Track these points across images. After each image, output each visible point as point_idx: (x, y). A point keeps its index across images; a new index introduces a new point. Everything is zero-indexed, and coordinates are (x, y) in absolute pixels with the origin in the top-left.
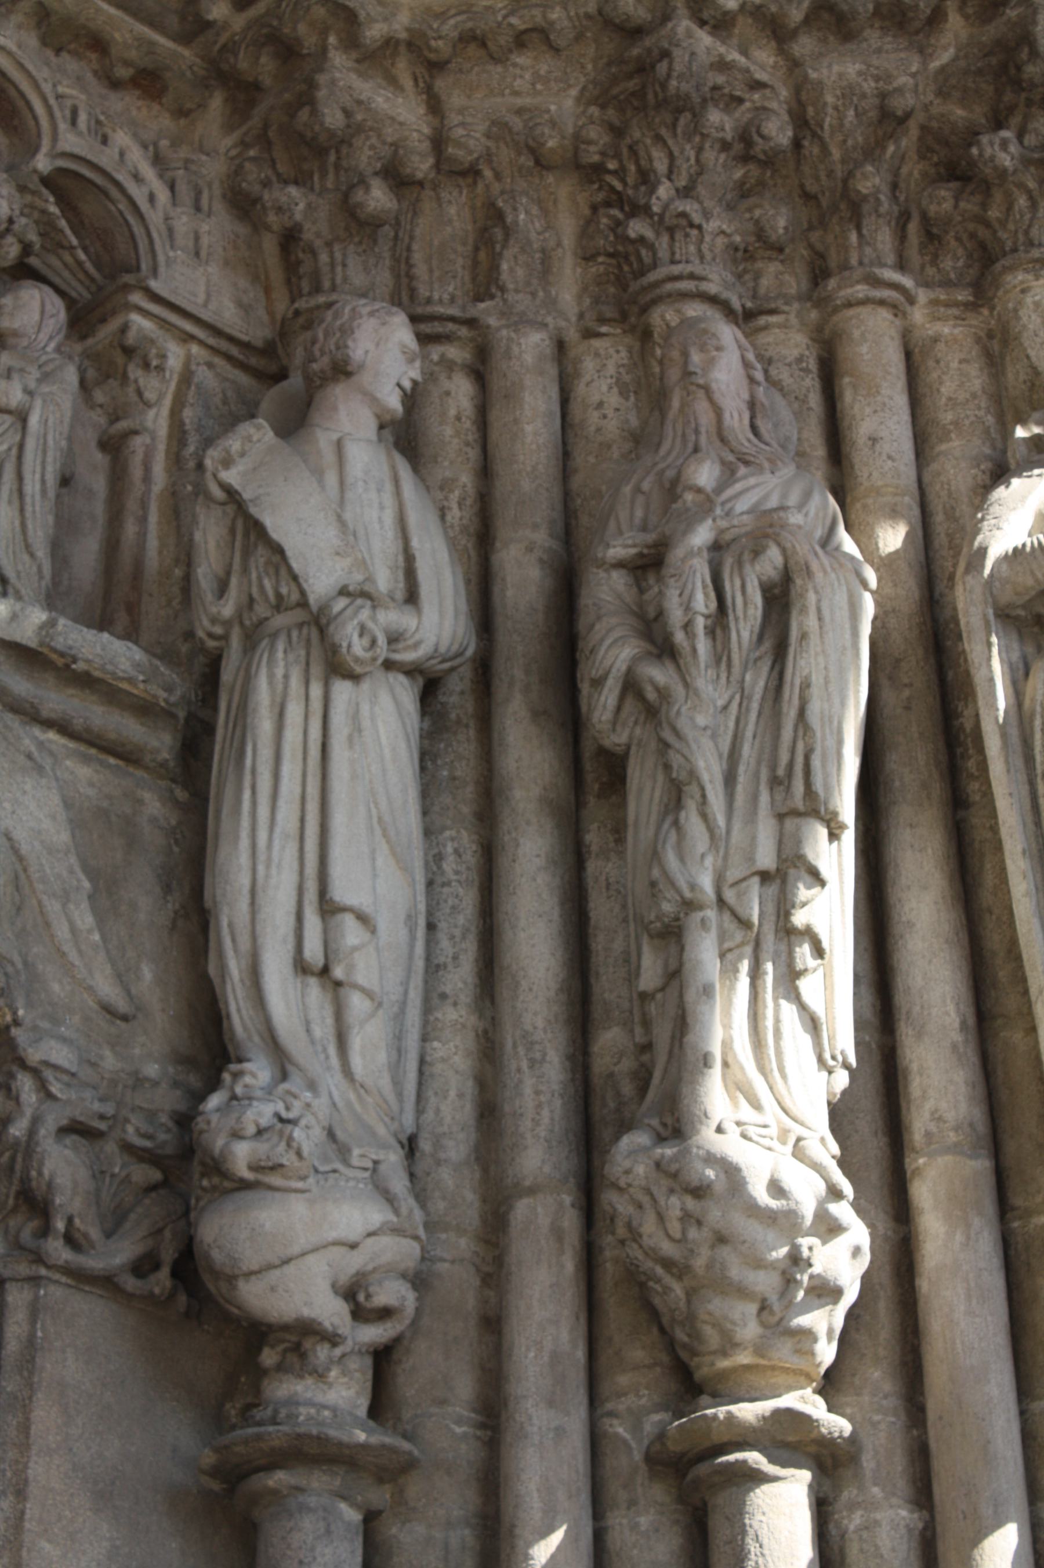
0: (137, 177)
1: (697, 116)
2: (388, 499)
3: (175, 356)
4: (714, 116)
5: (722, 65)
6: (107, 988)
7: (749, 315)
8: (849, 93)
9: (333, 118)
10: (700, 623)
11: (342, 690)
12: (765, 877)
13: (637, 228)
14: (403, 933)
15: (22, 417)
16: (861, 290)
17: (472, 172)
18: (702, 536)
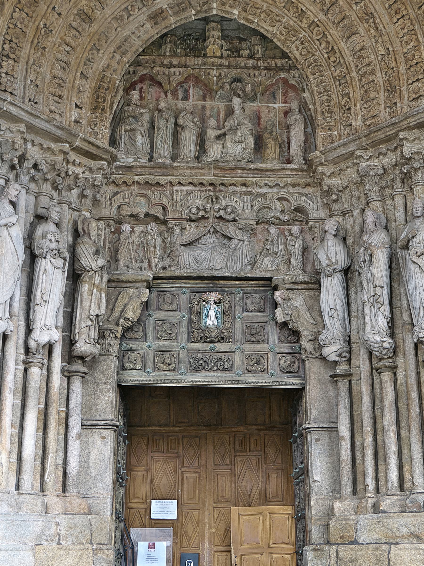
1: (369, 173)
2: (334, 248)
3: (317, 225)
4: (371, 173)
5: (369, 166)
7: (383, 199)
8: (388, 163)
9: (326, 188)
10: (362, 263)
11: (329, 278)
12: (374, 296)
13: (366, 192)
14: (341, 308)
15: (295, 246)
16: (395, 193)
17: (347, 187)
18: (363, 249)
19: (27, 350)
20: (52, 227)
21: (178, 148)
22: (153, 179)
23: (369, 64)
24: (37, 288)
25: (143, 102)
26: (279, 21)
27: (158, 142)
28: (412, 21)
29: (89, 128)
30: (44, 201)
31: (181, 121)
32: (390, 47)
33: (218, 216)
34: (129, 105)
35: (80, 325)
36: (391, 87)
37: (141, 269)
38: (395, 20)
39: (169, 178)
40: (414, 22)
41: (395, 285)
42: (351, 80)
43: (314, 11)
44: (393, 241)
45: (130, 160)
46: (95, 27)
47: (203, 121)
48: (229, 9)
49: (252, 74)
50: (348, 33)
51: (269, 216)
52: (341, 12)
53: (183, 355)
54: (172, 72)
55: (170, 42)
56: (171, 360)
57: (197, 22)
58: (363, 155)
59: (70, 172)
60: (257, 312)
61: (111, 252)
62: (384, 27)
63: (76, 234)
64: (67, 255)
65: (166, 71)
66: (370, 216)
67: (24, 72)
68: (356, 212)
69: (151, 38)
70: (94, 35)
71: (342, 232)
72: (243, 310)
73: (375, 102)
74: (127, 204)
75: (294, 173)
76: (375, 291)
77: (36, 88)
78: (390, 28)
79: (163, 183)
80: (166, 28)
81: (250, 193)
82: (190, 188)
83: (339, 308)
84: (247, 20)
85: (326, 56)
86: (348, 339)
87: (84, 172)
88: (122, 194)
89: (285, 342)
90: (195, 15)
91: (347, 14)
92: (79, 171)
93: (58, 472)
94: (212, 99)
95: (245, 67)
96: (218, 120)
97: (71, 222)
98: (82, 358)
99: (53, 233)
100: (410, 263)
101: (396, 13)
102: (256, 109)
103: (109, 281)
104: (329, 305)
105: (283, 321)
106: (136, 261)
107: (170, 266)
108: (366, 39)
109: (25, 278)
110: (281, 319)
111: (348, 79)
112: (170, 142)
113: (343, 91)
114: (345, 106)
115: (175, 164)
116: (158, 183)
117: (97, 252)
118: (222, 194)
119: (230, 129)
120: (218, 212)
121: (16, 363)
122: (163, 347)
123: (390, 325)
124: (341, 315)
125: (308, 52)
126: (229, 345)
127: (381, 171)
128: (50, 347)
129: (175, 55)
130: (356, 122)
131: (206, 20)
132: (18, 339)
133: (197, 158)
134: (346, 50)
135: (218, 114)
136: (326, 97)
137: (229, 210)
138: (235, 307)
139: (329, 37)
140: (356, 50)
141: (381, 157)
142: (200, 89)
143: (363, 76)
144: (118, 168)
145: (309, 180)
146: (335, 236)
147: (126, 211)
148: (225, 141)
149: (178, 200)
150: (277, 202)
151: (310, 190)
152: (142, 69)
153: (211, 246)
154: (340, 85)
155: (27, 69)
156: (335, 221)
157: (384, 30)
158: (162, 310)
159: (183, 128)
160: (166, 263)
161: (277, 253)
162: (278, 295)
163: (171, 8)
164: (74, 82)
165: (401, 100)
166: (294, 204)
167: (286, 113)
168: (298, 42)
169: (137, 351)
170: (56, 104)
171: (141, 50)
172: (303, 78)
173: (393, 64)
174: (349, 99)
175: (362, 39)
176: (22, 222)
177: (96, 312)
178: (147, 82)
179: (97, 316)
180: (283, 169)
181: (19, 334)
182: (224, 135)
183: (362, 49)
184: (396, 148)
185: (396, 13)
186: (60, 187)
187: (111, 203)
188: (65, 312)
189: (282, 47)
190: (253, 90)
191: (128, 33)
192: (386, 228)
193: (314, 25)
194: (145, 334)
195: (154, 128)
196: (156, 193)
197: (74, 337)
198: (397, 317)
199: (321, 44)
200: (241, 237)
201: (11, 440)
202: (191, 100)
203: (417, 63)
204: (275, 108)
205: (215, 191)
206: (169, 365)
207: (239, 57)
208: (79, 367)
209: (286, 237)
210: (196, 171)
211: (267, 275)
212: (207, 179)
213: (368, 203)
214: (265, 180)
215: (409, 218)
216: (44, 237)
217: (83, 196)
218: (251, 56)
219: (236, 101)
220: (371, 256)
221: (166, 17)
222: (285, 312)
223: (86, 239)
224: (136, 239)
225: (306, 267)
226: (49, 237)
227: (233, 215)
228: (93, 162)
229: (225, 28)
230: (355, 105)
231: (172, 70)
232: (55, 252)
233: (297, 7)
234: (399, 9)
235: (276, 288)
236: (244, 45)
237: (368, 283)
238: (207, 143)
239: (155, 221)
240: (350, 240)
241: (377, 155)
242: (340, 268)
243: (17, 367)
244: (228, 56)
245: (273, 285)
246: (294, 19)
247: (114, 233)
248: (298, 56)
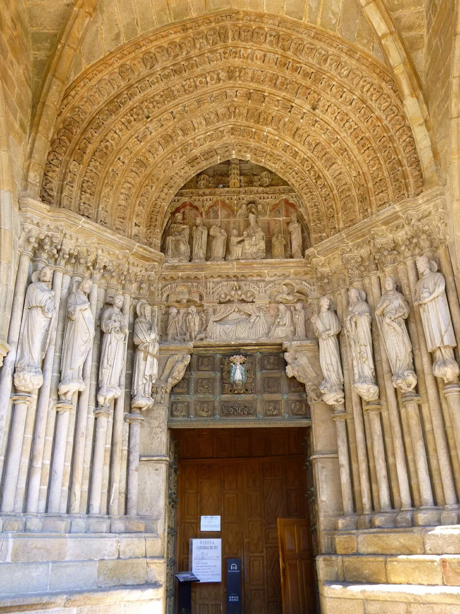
0: (306, 286)
4: (352, 261)
6: (314, 374)
8: (364, 253)
9: (319, 275)
12: (360, 353)
18: (349, 317)
20: (116, 310)
21: (211, 252)
22: (193, 274)
23: (346, 184)
24: (104, 356)
25: (185, 221)
26: (279, 160)
27: (196, 248)
28: (375, 151)
29: (145, 240)
31: (212, 233)
32: (360, 170)
33: (240, 299)
34: (175, 223)
35: (138, 383)
36: (362, 198)
37: (184, 340)
38: (363, 151)
39: (203, 273)
40: (376, 151)
41: (376, 344)
42: (334, 196)
43: (304, 151)
44: (372, 311)
45: (175, 262)
46: (149, 169)
47: (228, 231)
48: (244, 154)
49: (262, 198)
50: (329, 164)
52: (323, 149)
54: (205, 199)
55: (204, 179)
56: (208, 409)
57: (223, 165)
58: (345, 248)
59: (130, 271)
60: (272, 369)
61: (162, 328)
62: (355, 157)
63: (135, 316)
64: (127, 331)
65: (201, 198)
66: (353, 294)
67: (98, 202)
68: (343, 291)
69: (189, 176)
70: (148, 176)
71: (333, 307)
72: (262, 368)
73: (351, 210)
74: (174, 293)
75: (295, 264)
76: (360, 349)
77: (106, 213)
78: (359, 158)
79: (200, 277)
80: (200, 169)
81: (264, 281)
82: (219, 279)
83: (334, 363)
84: (257, 161)
85: (314, 181)
86: (342, 387)
87: (141, 271)
88: (170, 286)
89: (295, 392)
90: (220, 159)
91: (328, 150)
92: (137, 270)
93: (121, 497)
94: (235, 216)
95: (257, 192)
96: (239, 231)
97: (132, 307)
98: (140, 408)
99: (116, 314)
100: (386, 326)
101: (363, 146)
102: (266, 222)
103: (160, 350)
104: (326, 362)
105: (292, 375)
106: (181, 334)
107: (206, 337)
108: (342, 167)
109: (96, 349)
110: (290, 375)
111: (331, 195)
112: (204, 248)
113: (328, 204)
114: (330, 215)
115: (208, 263)
116: (196, 277)
117: (150, 328)
118: (243, 282)
119: (248, 236)
120: (241, 296)
121: (88, 413)
122: (203, 398)
123: (374, 374)
124: (336, 369)
125: (302, 179)
126: (252, 395)
127: (360, 260)
128: (116, 401)
129: (208, 187)
130: (339, 225)
131: (228, 163)
132: (90, 395)
134: (328, 175)
135: (239, 227)
136: (316, 210)
137: (249, 294)
138: (255, 365)
139: (316, 167)
140: (335, 175)
141: (359, 249)
142: (226, 210)
143: (342, 191)
144: (167, 268)
145: (306, 269)
146: (328, 309)
147: (173, 298)
148: (244, 245)
149: (211, 289)
150: (284, 286)
151: (307, 277)
152: (183, 198)
153: (236, 321)
154: (326, 200)
155: (99, 200)
156: (328, 298)
157: (355, 159)
158: (201, 370)
159: (214, 237)
160: (202, 335)
161: (285, 324)
162: (288, 356)
163: (203, 155)
164: (134, 208)
165: (371, 207)
166: (297, 288)
167: (288, 224)
168: (294, 173)
169: (183, 402)
170: (120, 224)
171: (182, 185)
172: (299, 197)
173: (363, 182)
174: (333, 209)
175: (340, 167)
176: (94, 308)
177: (150, 373)
178: (188, 207)
179: (151, 376)
180: (288, 262)
181: (91, 391)
182: (243, 241)
183: (340, 174)
184: (369, 242)
185: (363, 146)
186: (123, 282)
187: (162, 293)
188: (127, 374)
189: (282, 177)
190: (263, 208)
191: (173, 174)
192: (366, 301)
193: (304, 161)
194: (188, 389)
195: (193, 238)
196: (194, 284)
197: (134, 393)
198: (379, 369)
199: (310, 173)
200: (258, 314)
201: (83, 474)
202: (220, 218)
203: (381, 180)
204: (280, 221)
205: (237, 281)
206: (207, 412)
207: (253, 186)
208: (137, 416)
209: (291, 312)
210: (223, 267)
211: (279, 341)
212: (231, 273)
213: (351, 283)
214: (275, 271)
215: (383, 293)
216: (110, 318)
217: (140, 288)
218: (261, 186)
219: (252, 217)
220: (356, 323)
221: (200, 162)
222: (293, 368)
223: (142, 319)
224: (181, 319)
225: (308, 334)
226: (113, 318)
227: (252, 298)
228: (148, 263)
229: (243, 168)
230: (337, 214)
231: (205, 197)
232: (118, 329)
233: (292, 149)
234: (365, 144)
235: (285, 351)
236: (256, 178)
237: (355, 343)
238: (231, 247)
239: (194, 305)
240: (339, 312)
241: (356, 248)
242: (332, 334)
243: (89, 416)
244: (245, 186)
245: (283, 349)
246: (290, 157)
247: (165, 314)
248: (294, 183)
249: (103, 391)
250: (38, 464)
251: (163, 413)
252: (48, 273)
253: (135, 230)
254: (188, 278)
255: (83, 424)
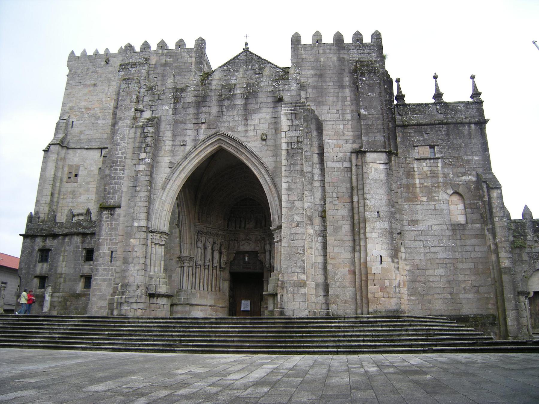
19: (213, 267)
30: (215, 239)
45: (231, 229)
51: (258, 239)
53: (242, 267)
63: (221, 245)
98: (222, 268)
117: (225, 248)
133: (244, 228)
208: (222, 269)
217: (222, 237)
219: (252, 215)
235: (258, 253)
249: (214, 265)
250: (201, 281)
251: (228, 268)
252: (201, 239)
253: (220, 222)
254: (235, 234)
255: (210, 272)
